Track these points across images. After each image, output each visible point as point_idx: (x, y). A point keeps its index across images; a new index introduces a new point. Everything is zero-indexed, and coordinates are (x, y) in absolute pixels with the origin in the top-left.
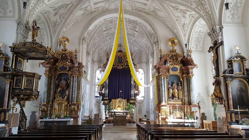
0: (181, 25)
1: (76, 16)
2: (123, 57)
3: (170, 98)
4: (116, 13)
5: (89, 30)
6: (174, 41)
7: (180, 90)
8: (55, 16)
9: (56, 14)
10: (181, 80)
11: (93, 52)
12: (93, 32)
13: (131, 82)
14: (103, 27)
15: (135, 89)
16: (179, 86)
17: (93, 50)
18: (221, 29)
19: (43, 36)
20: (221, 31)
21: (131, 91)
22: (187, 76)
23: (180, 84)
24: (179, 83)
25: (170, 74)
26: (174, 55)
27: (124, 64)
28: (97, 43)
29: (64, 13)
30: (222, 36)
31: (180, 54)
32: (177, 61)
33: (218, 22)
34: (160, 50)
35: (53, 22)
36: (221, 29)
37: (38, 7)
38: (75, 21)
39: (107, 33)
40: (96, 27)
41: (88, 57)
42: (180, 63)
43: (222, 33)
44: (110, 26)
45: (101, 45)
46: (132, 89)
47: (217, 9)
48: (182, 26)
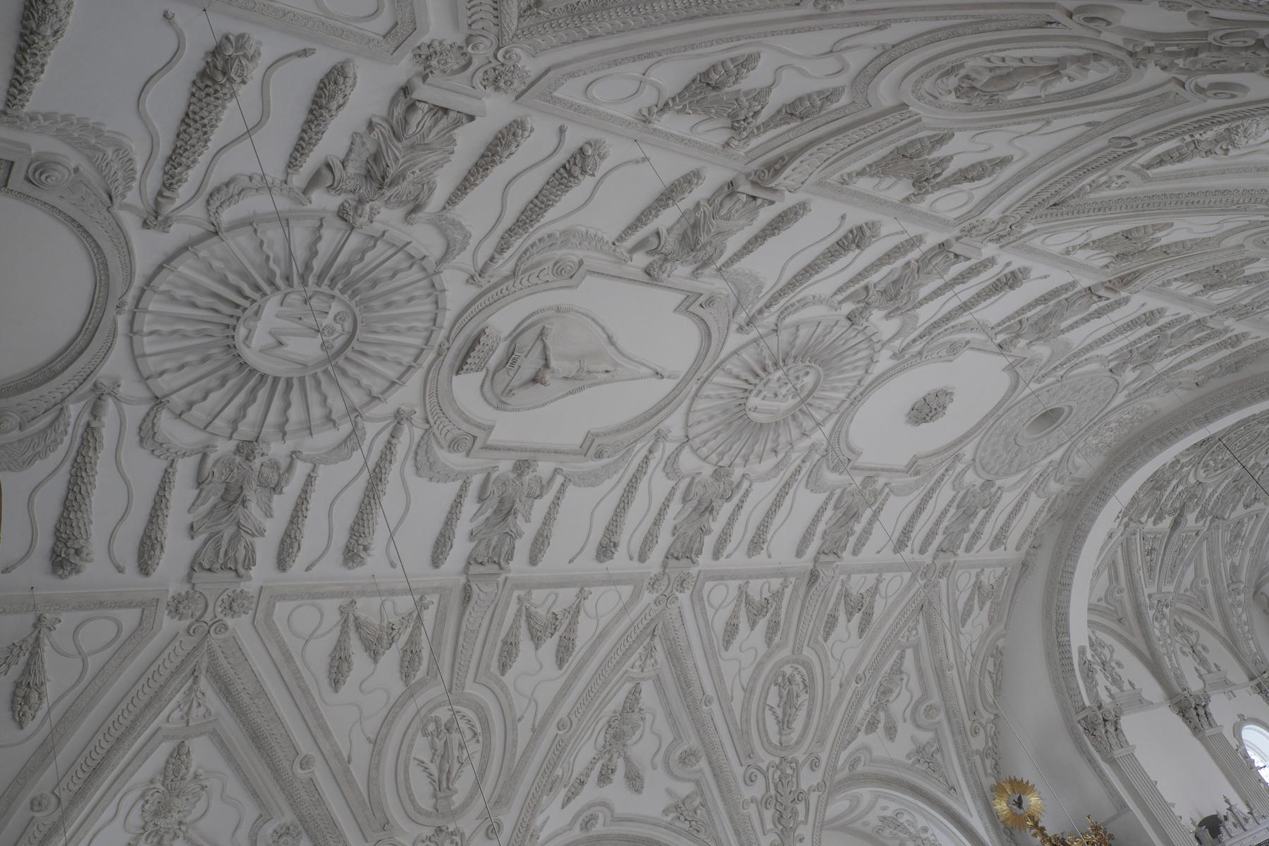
1: (973, 656)
4: (1131, 474)
5: (1082, 651)
8: (896, 739)
9: (891, 731)
11: (1224, 641)
12: (1121, 591)
14: (1149, 525)
17: (1214, 632)
19: (924, 836)
28: (1205, 582)
29: (917, 695)
35: (910, 762)
37: (801, 831)
38: (990, 667)
39: (1201, 516)
40: (1114, 563)
41: (1209, 732)
44: (1181, 488)
45: (1235, 569)
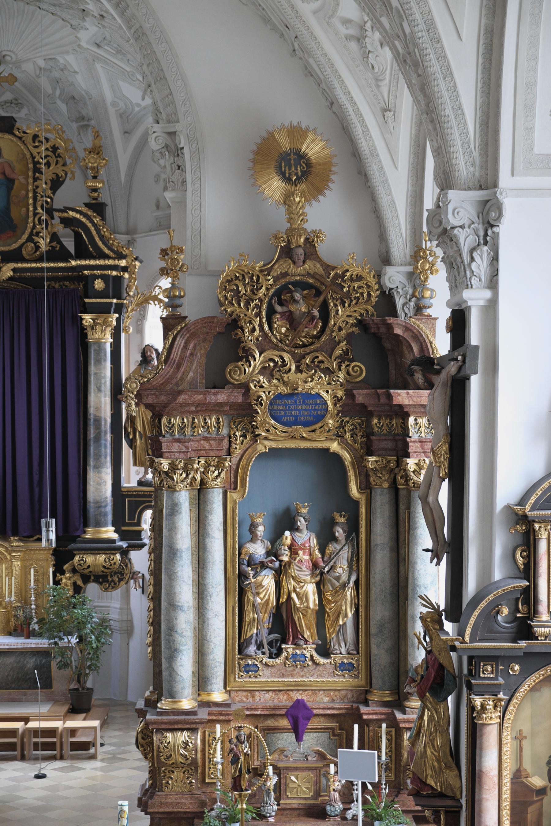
0: (343, 31)
2: (21, 179)
3: (252, 649)
6: (301, 156)
7: (338, 579)
10: (354, 491)
13: (92, 398)
15: (126, 452)
16: (332, 547)
20: (486, 235)
21: (91, 475)
22: (392, 470)
23: (339, 532)
24: (333, 523)
25: (263, 447)
26: (301, 285)
27: (30, 239)
31: (355, 270)
32: (322, 331)
33: (476, 154)
34: (164, 252)
42: (346, 353)
43: (495, 259)
46: (98, 456)
48: (348, 38)
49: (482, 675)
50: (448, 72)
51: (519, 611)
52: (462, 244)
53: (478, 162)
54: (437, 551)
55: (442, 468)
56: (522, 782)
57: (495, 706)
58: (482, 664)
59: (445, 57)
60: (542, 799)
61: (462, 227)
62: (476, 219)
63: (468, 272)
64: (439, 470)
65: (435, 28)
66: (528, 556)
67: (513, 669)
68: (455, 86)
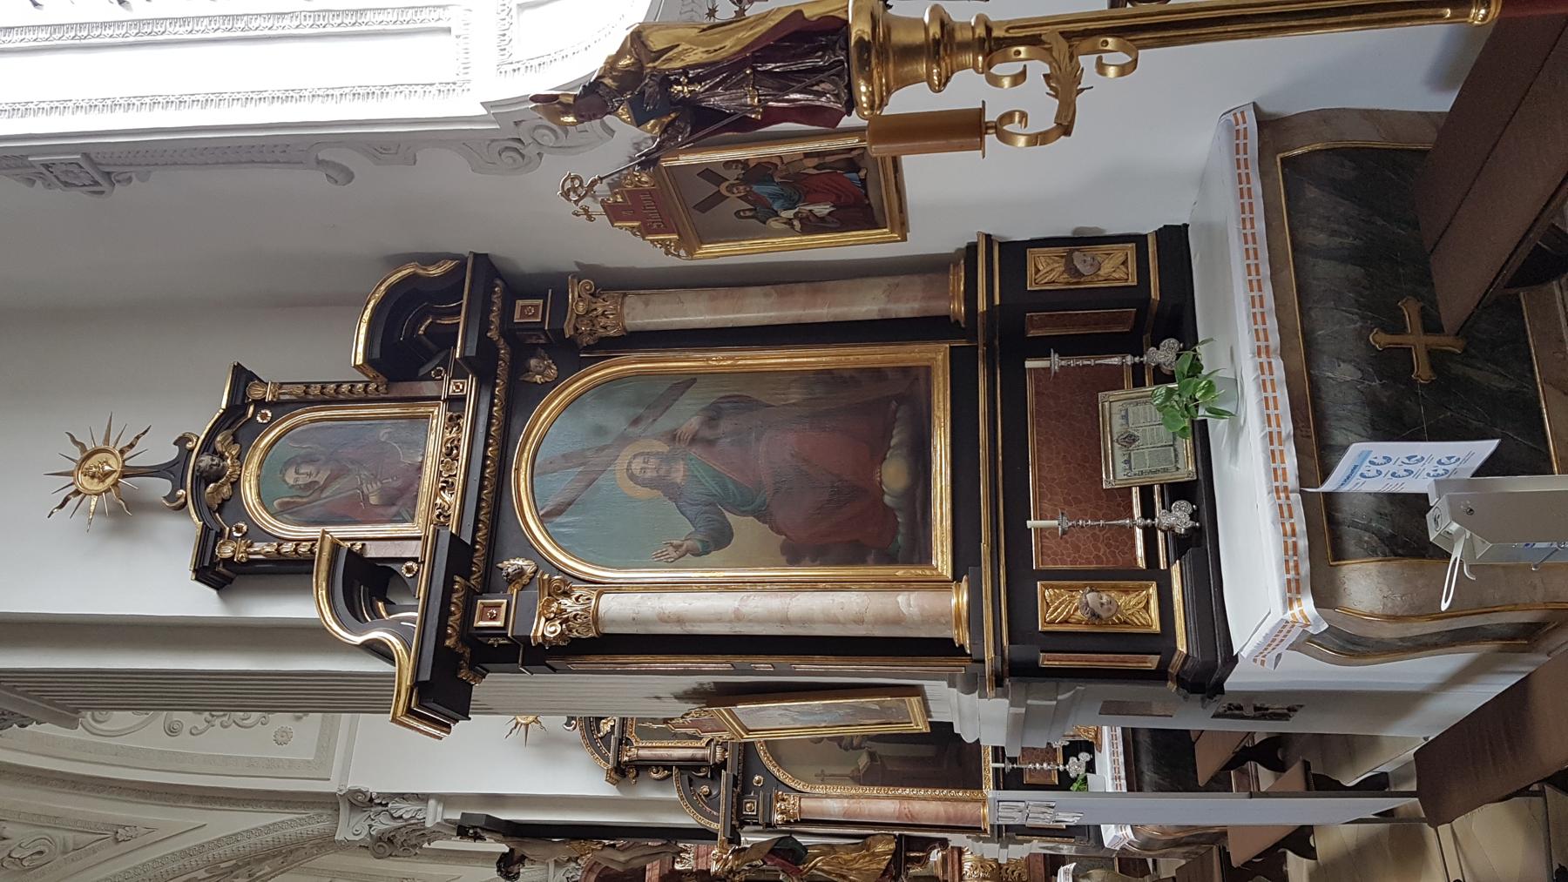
18: (371, 800)
20: (380, 804)
30: (423, 798)
36: (362, 802)
43: (403, 797)
47: (205, 825)
49: (755, 813)
50: (234, 837)
51: (706, 776)
52: (387, 827)
53: (320, 811)
54: (673, 853)
55: (593, 847)
56: (863, 775)
57: (783, 800)
58: (744, 813)
59: (219, 840)
60: (880, 757)
61: (370, 826)
62: (367, 814)
63: (412, 822)
64: (596, 849)
65: (189, 849)
66: (657, 766)
67: (758, 782)
68: (247, 831)
